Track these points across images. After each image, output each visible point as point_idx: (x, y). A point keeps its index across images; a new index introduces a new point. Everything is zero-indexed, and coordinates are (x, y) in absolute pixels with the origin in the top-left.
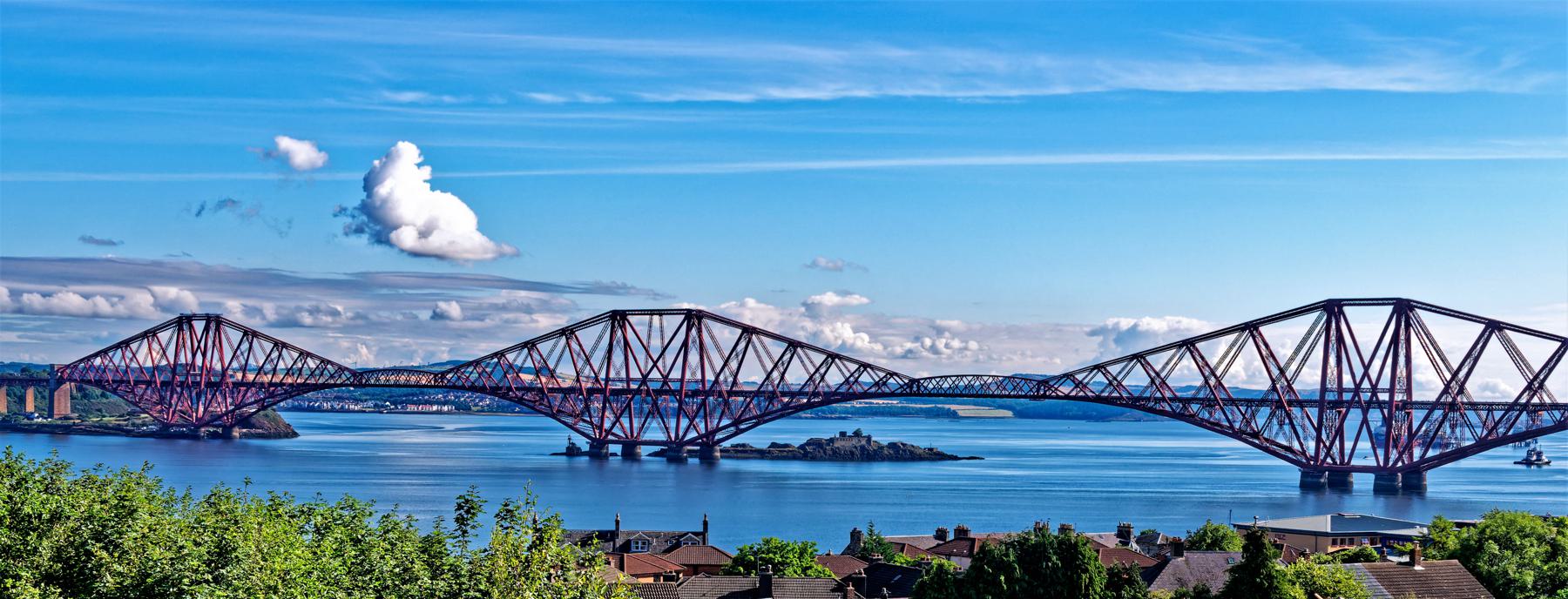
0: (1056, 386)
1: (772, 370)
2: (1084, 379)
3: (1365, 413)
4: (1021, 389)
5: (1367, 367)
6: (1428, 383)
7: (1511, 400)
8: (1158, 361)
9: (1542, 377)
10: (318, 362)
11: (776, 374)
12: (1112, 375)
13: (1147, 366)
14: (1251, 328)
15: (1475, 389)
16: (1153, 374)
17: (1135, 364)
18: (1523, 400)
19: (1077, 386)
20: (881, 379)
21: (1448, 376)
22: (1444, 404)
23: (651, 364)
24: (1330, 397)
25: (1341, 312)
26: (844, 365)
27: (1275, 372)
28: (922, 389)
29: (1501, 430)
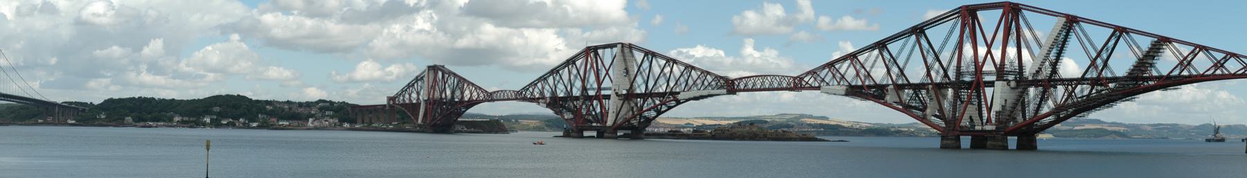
10: (699, 73)
16: (858, 67)
19: (815, 79)
25: (975, 17)
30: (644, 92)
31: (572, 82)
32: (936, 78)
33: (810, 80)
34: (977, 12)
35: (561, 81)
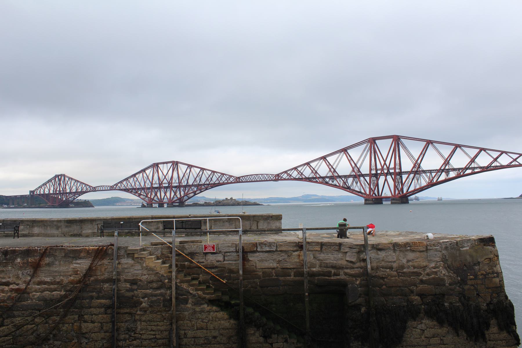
0: (281, 176)
1: (196, 178)
2: (290, 173)
3: (386, 177)
4: (271, 178)
5: (385, 161)
6: (407, 165)
7: (438, 168)
8: (313, 165)
9: (448, 160)
11: (198, 179)
12: (299, 171)
13: (310, 167)
14: (345, 150)
15: (425, 166)
16: (312, 169)
17: (306, 167)
18: (442, 168)
19: (288, 175)
20: (228, 178)
21: (415, 162)
22: (413, 172)
23: (164, 177)
24: (373, 172)
25: (375, 143)
26: (217, 174)
27: (353, 165)
28: (240, 180)
29: (435, 181)
30: (69, 192)
31: (145, 181)
32: (147, 186)
33: (285, 176)
34: (376, 141)
35: (137, 181)
